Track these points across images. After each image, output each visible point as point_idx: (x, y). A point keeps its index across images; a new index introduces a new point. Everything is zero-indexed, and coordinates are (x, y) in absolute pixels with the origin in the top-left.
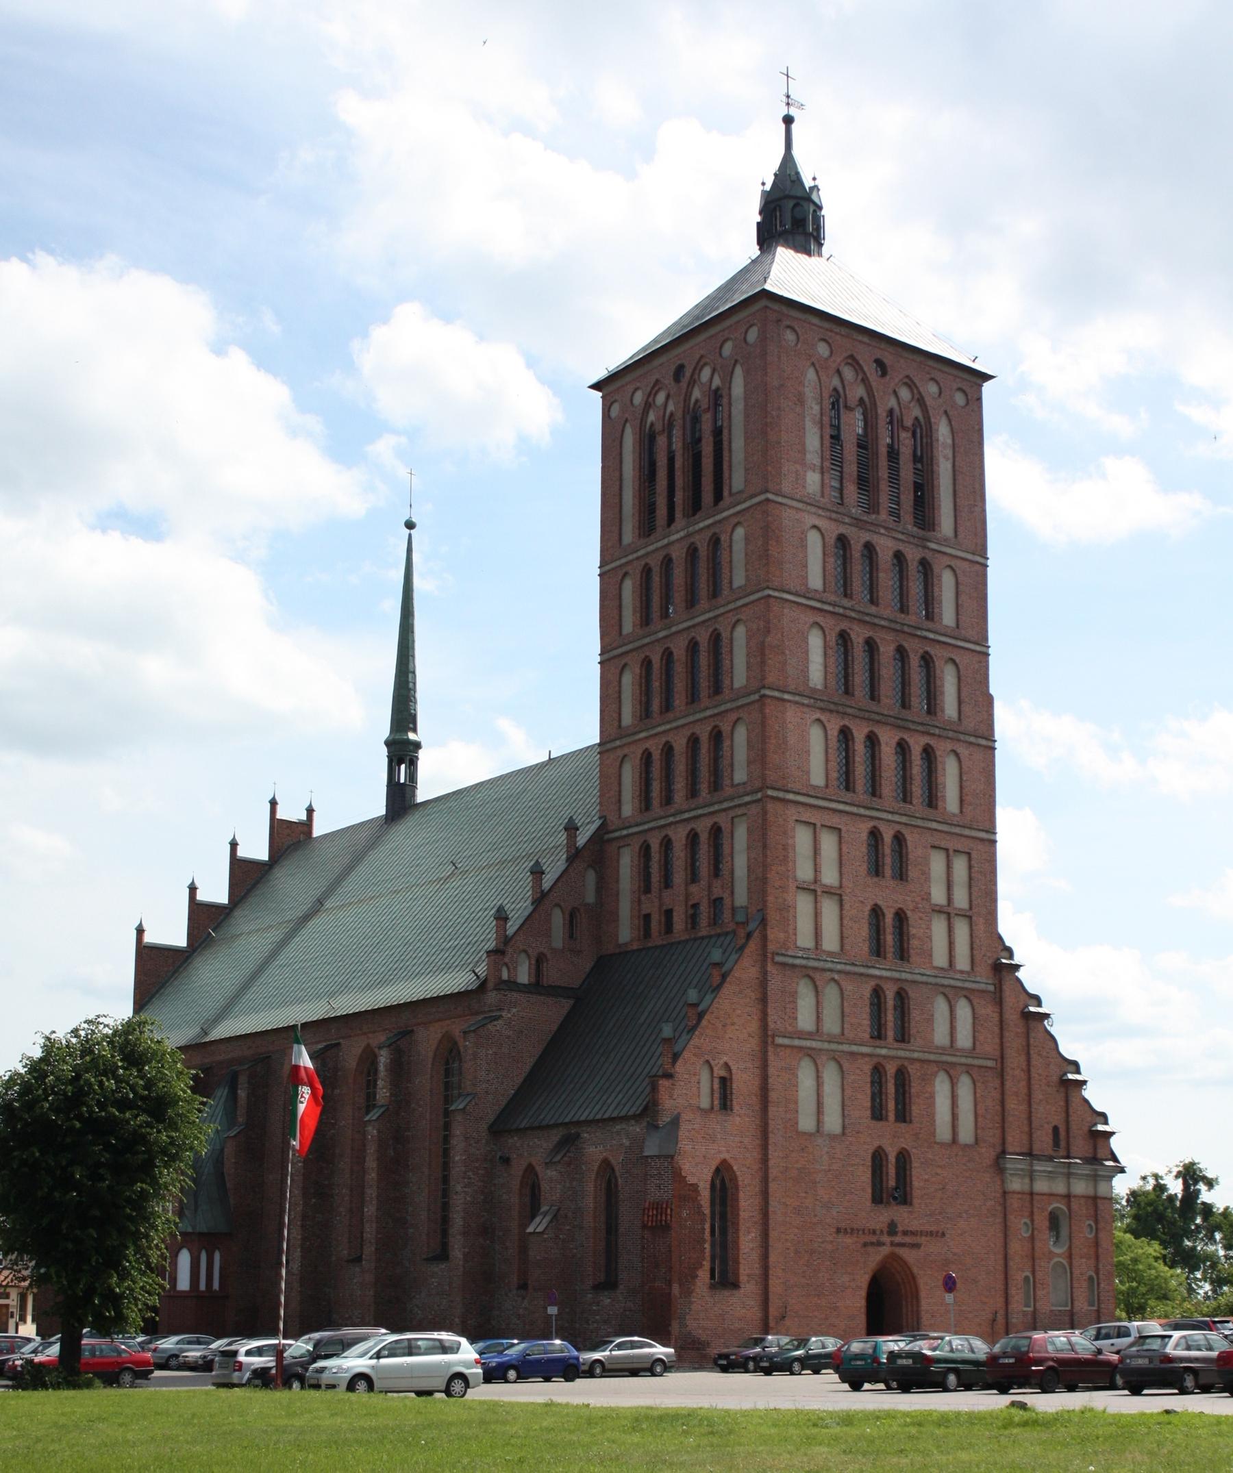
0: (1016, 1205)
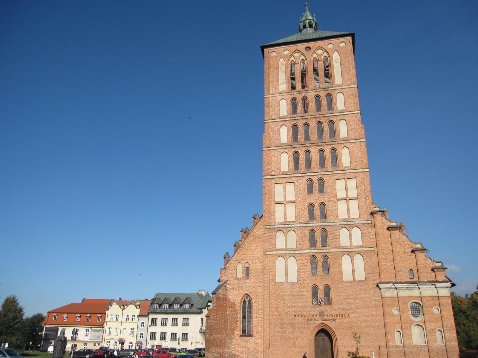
0: (388, 302)
